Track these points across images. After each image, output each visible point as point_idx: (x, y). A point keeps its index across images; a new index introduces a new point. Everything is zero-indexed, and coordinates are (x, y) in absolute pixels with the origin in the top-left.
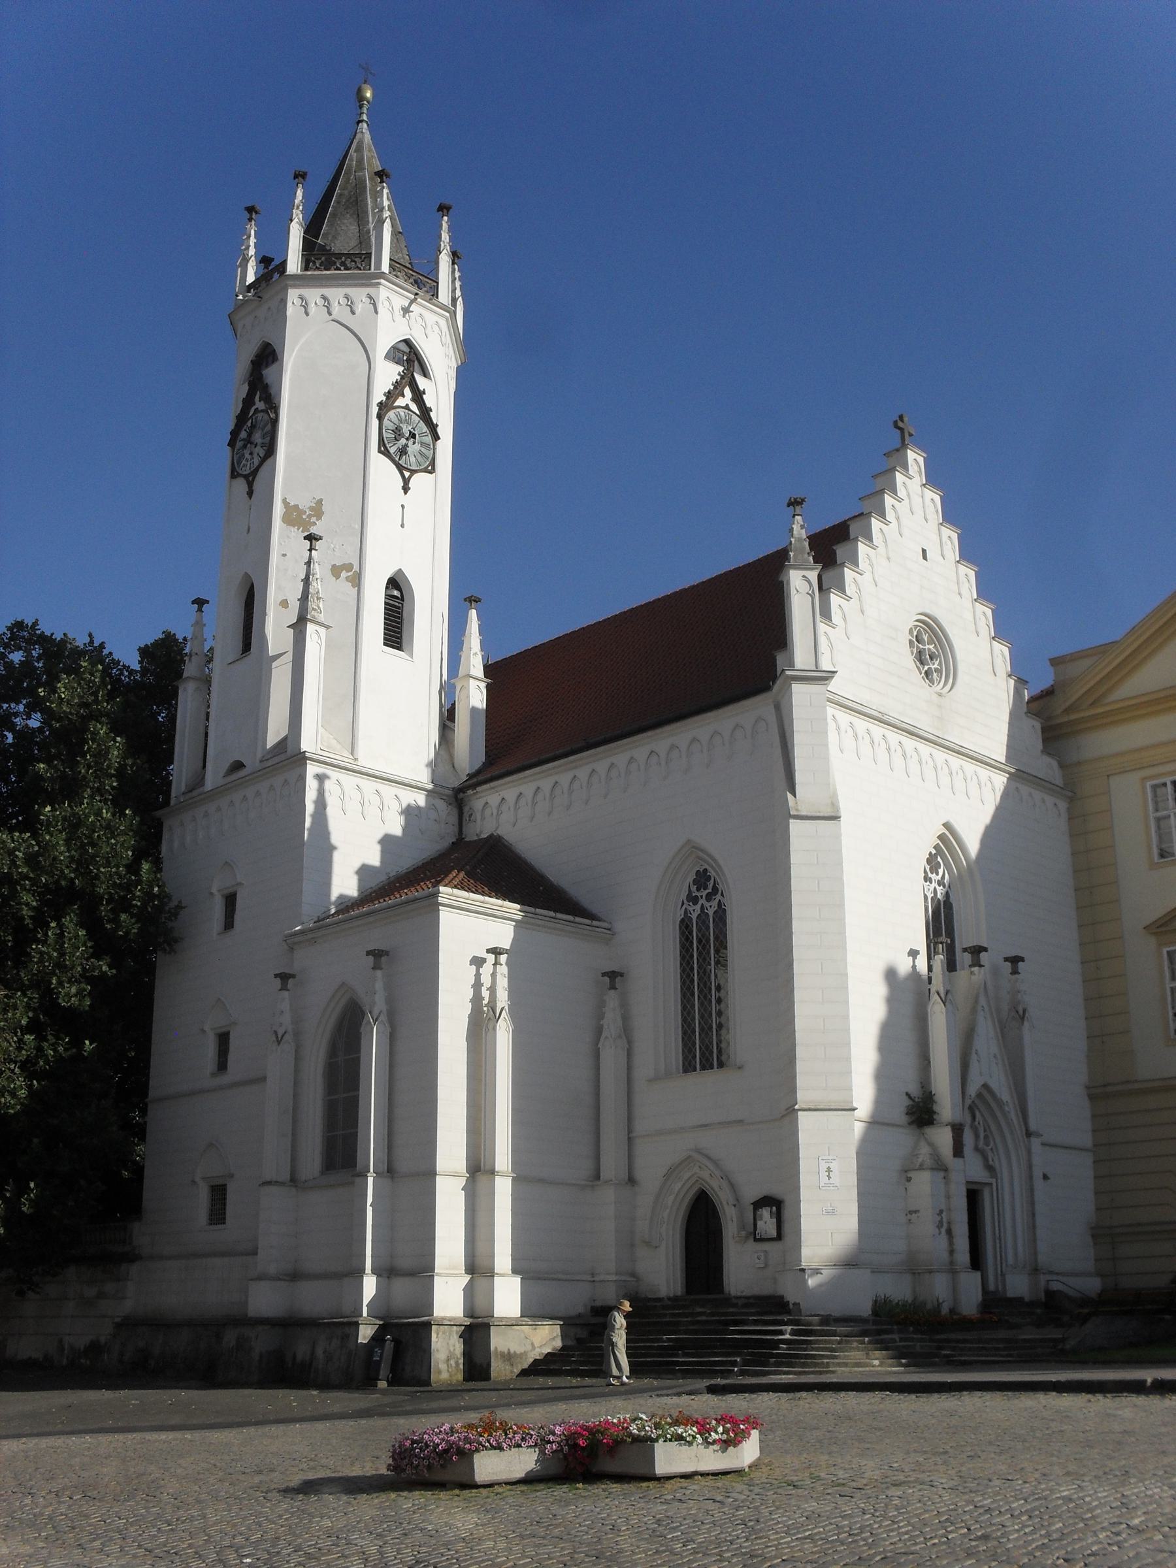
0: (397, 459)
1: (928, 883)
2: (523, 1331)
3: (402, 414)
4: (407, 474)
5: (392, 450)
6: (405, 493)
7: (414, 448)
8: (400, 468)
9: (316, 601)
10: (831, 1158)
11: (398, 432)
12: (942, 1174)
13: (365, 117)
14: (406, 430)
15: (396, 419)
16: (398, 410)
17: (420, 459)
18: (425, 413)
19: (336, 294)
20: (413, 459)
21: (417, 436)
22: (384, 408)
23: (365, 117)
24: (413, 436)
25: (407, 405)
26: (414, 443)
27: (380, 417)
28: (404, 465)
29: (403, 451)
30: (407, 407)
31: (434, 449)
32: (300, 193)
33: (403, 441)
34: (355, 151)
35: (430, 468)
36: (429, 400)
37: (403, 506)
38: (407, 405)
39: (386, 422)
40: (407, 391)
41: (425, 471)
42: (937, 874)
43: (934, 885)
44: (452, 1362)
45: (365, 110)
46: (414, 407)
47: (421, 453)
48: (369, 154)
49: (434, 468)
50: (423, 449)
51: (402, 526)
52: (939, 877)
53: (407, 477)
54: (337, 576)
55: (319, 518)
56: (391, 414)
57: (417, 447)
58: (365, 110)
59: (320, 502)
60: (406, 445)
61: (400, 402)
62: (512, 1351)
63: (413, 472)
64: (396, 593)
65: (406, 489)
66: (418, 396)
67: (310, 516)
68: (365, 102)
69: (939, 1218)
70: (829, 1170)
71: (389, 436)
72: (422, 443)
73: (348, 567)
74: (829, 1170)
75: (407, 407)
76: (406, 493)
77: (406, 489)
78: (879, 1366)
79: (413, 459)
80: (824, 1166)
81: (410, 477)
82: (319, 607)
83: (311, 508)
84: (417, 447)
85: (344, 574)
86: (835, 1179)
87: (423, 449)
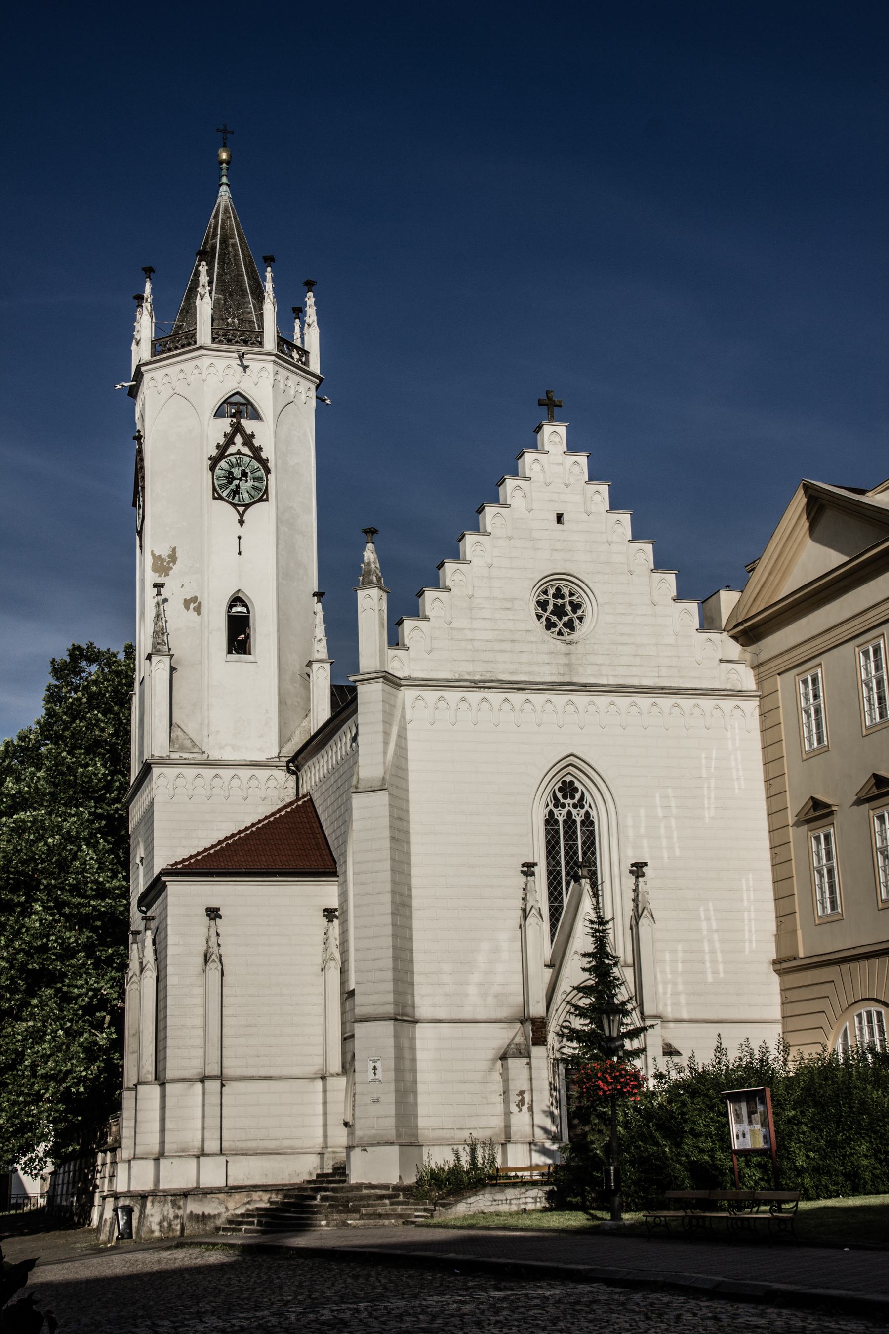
0: (230, 500)
1: (560, 808)
2: (218, 1198)
3: (233, 460)
4: (241, 509)
5: (224, 494)
6: (242, 525)
7: (246, 486)
8: (235, 506)
9: (160, 636)
10: (376, 1058)
11: (230, 477)
12: (526, 1060)
13: (224, 180)
14: (237, 472)
15: (227, 466)
16: (228, 458)
17: (253, 492)
18: (256, 452)
19: (173, 370)
20: (246, 495)
21: (249, 474)
22: (215, 462)
23: (224, 180)
24: (245, 474)
25: (239, 450)
26: (247, 481)
27: (212, 469)
28: (237, 503)
29: (236, 492)
30: (239, 452)
31: (267, 480)
32: (148, 287)
33: (236, 482)
34: (214, 218)
35: (265, 497)
36: (256, 442)
37: (239, 538)
38: (239, 450)
39: (217, 471)
40: (238, 439)
41: (261, 500)
42: (573, 798)
43: (567, 809)
44: (165, 1224)
45: (224, 172)
46: (246, 450)
47: (254, 488)
48: (224, 218)
49: (267, 497)
50: (256, 484)
51: (240, 553)
52: (576, 801)
53: (243, 508)
54: (187, 608)
55: (174, 563)
56: (223, 464)
57: (250, 483)
58: (224, 172)
59: (174, 550)
60: (238, 486)
61: (232, 449)
62: (206, 1213)
63: (247, 506)
64: (239, 609)
65: (241, 522)
66: (248, 440)
67: (169, 563)
68: (224, 165)
69: (520, 1098)
70: (375, 1068)
71: (222, 482)
72: (254, 479)
73: (194, 600)
74: (375, 1068)
75: (239, 452)
76: (242, 525)
77: (241, 522)
78: (610, 1220)
79: (246, 495)
80: (371, 1065)
81: (244, 512)
82: (163, 641)
83: (169, 556)
84: (250, 483)
85: (192, 606)
86: (379, 1075)
87: (256, 484)
